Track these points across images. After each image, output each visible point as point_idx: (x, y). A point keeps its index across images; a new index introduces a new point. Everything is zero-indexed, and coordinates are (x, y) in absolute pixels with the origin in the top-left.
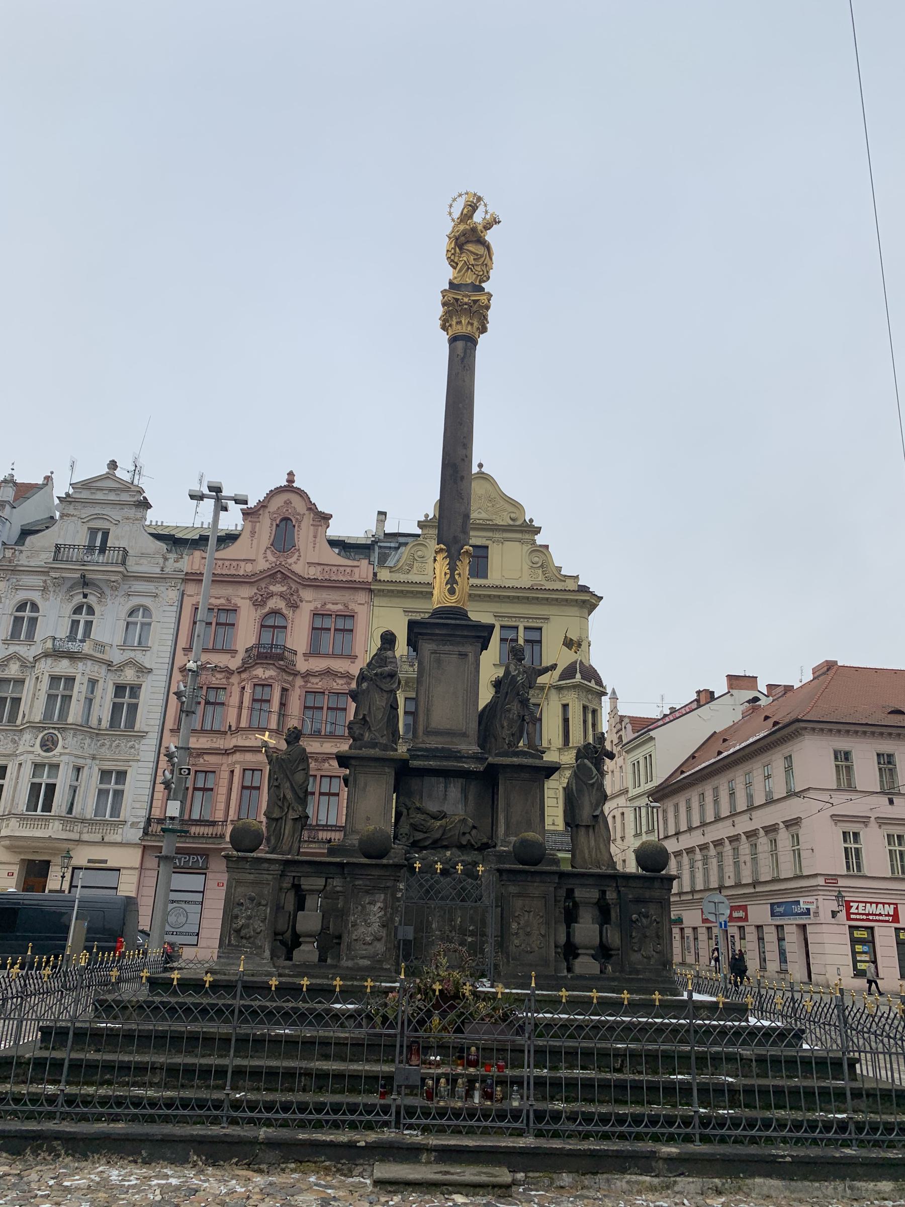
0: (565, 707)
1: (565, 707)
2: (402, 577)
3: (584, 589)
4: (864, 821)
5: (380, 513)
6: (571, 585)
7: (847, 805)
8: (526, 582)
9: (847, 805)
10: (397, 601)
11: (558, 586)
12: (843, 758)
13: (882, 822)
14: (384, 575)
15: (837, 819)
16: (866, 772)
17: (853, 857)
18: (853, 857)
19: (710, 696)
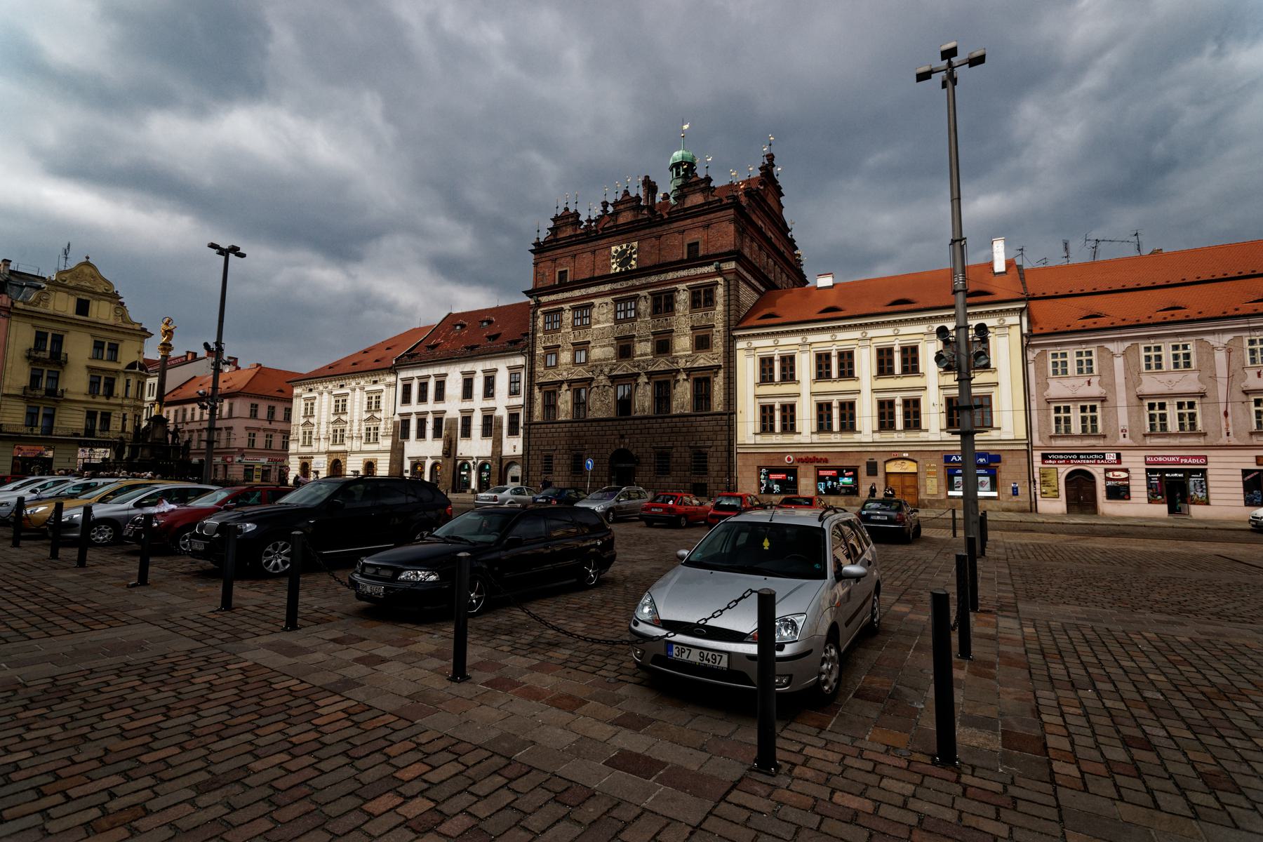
0: (128, 381)
1: (128, 381)
2: (32, 308)
3: (144, 330)
4: (258, 429)
5: (4, 260)
6: (137, 327)
7: (253, 423)
8: (111, 321)
9: (253, 423)
10: (26, 320)
11: (130, 326)
12: (254, 408)
13: (265, 430)
14: (20, 305)
15: (247, 428)
16: (263, 412)
17: (252, 442)
18: (252, 442)
19: (195, 357)
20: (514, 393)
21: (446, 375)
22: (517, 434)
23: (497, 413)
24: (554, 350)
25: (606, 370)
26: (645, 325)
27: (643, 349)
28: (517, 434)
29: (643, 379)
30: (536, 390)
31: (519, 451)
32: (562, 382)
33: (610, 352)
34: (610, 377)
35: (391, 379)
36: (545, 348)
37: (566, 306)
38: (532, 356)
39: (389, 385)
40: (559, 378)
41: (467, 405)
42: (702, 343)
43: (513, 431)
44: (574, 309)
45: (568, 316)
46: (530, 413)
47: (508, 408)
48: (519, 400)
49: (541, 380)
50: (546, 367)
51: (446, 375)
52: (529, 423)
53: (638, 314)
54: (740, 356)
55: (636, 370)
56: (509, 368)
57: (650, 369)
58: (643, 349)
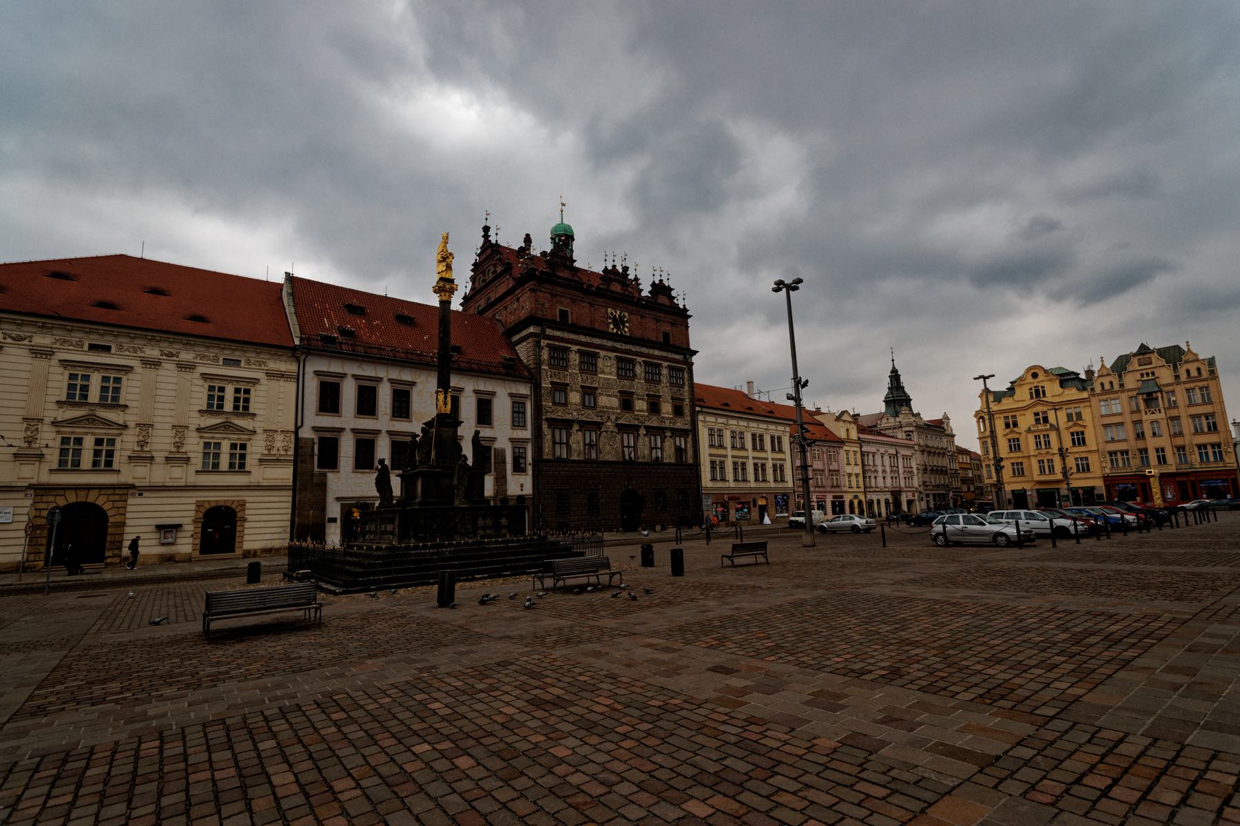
20: (518, 422)
21: (413, 384)
22: (524, 471)
23: (497, 445)
24: (562, 388)
25: (613, 417)
26: (639, 386)
27: (641, 405)
28: (524, 471)
29: (642, 431)
30: (545, 426)
31: (528, 490)
32: (573, 421)
33: (615, 402)
34: (618, 425)
35: (290, 367)
36: (552, 383)
37: (575, 348)
38: (537, 388)
39: (282, 375)
40: (569, 417)
41: (328, 421)
42: (678, 411)
43: (518, 468)
44: (579, 351)
45: (574, 358)
46: (538, 449)
47: (512, 440)
48: (527, 434)
49: (549, 415)
50: (554, 404)
51: (413, 384)
52: (538, 461)
53: (635, 376)
54: (700, 424)
55: (636, 423)
56: (511, 395)
57: (647, 424)
58: (641, 405)
